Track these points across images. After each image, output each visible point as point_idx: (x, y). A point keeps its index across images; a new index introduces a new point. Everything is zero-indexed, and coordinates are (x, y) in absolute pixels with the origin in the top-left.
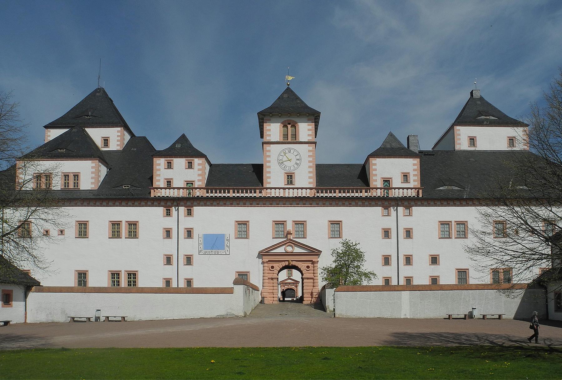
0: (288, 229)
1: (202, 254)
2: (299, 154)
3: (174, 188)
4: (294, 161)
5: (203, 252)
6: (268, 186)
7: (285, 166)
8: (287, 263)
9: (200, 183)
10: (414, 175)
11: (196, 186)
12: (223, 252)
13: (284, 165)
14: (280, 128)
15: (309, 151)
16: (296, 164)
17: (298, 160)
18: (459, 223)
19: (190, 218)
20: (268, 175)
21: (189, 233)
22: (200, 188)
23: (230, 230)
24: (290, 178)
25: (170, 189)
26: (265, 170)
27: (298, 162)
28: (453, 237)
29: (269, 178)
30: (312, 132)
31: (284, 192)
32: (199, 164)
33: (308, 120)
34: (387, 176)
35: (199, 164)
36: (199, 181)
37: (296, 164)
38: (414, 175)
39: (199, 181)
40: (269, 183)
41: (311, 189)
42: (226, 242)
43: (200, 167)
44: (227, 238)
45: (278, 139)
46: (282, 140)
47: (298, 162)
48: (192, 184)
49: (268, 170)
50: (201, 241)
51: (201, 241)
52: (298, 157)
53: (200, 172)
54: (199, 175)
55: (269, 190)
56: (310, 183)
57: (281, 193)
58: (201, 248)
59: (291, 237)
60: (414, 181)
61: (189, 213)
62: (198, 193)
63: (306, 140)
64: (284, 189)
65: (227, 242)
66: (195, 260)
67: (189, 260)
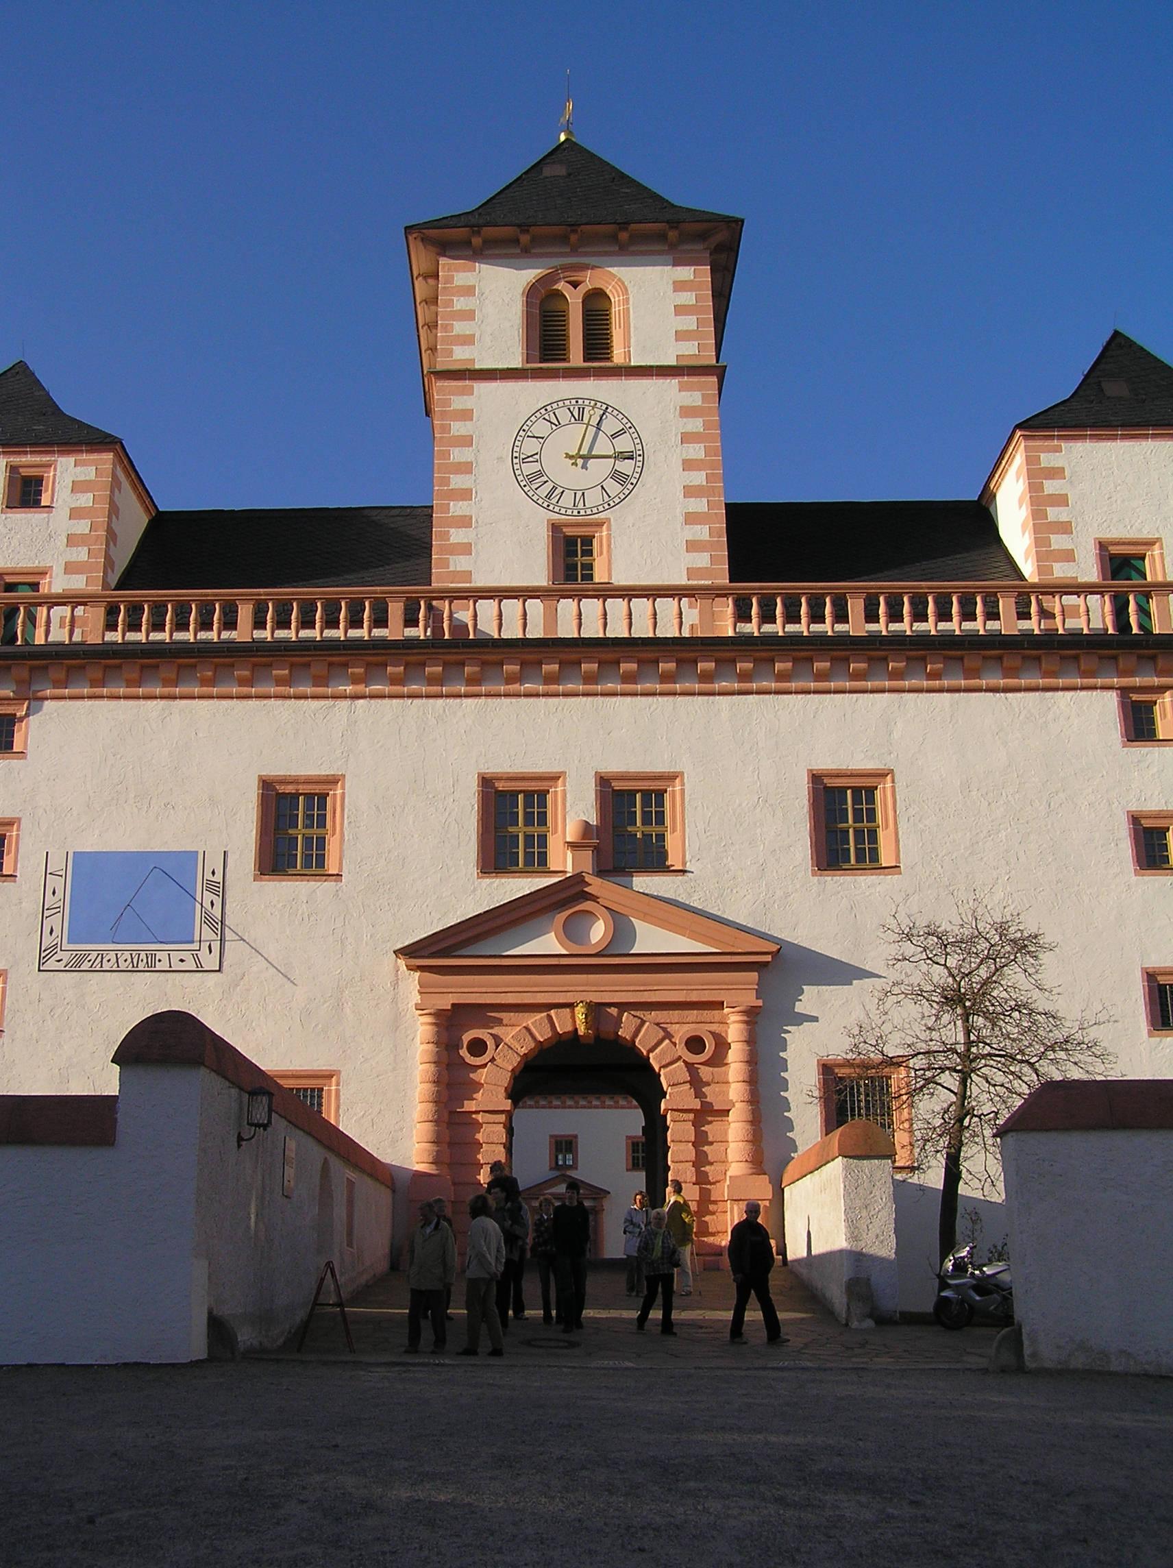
1: (61, 966)
5: (66, 956)
7: (554, 489)
12: (183, 955)
13: (550, 485)
15: (686, 412)
16: (617, 476)
20: (457, 536)
27: (626, 467)
30: (700, 322)
32: (77, 487)
34: (1122, 530)
35: (77, 487)
36: (70, 568)
37: (617, 476)
39: (70, 568)
40: (468, 575)
44: (208, 876)
45: (517, 362)
50: (60, 894)
51: (60, 894)
58: (57, 932)
65: (208, 897)
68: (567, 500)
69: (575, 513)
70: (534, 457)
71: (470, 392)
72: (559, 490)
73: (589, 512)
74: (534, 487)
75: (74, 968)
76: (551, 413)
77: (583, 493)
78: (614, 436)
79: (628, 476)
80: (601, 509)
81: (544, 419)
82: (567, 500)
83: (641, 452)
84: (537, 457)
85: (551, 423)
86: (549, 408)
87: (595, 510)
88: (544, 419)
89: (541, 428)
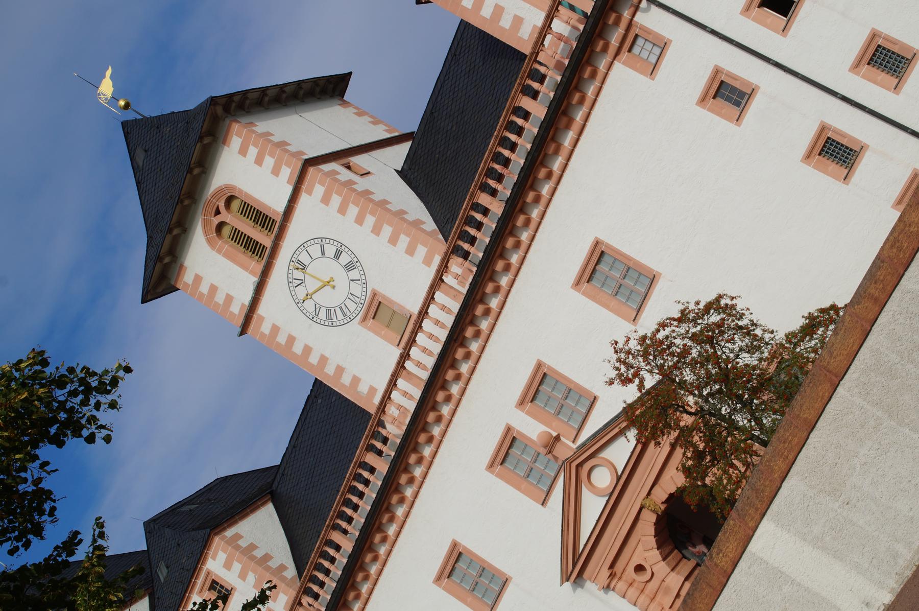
0: (534, 436)
2: (322, 241)
6: (377, 400)
8: (649, 518)
13: (338, 310)
14: (219, 251)
15: (326, 200)
16: (349, 267)
17: (338, 255)
27: (345, 259)
31: (411, 377)
33: (228, 146)
35: (228, 565)
40: (372, 390)
45: (251, 281)
46: (259, 268)
47: (345, 259)
52: (330, 250)
55: (392, 410)
59: (568, 446)
63: (289, 189)
68: (352, 306)
69: (361, 306)
71: (262, 319)
72: (343, 306)
73: (364, 298)
74: (335, 319)
76: (294, 281)
77: (351, 294)
78: (323, 253)
79: (351, 261)
80: (364, 290)
81: (296, 287)
82: (352, 306)
83: (340, 244)
84: (317, 306)
85: (300, 284)
86: (290, 280)
87: (364, 294)
88: (296, 287)
89: (301, 292)
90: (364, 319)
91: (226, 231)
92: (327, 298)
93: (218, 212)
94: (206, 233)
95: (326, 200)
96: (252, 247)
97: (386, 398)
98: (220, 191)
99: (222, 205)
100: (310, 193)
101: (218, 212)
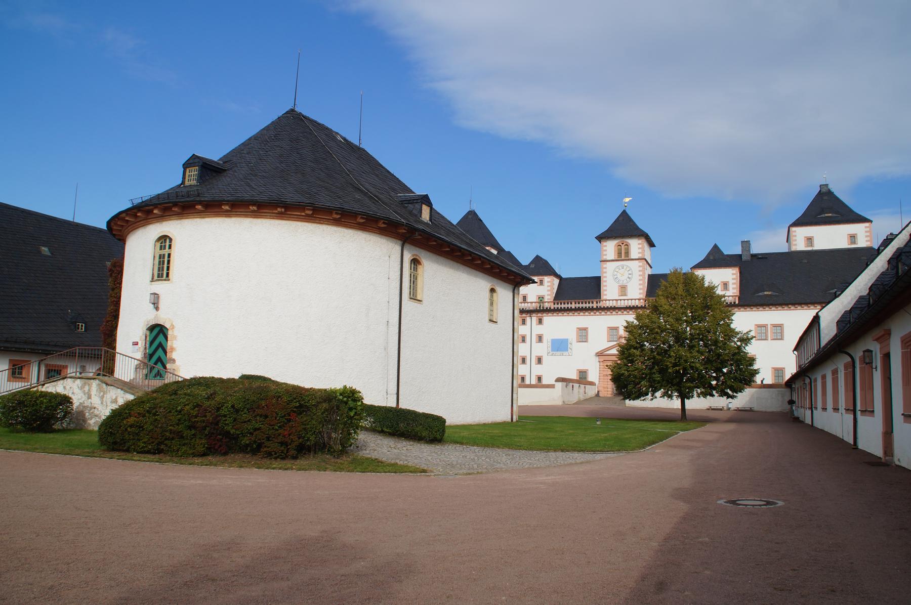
0: (620, 333)
3: (528, 303)
4: (626, 275)
9: (549, 297)
10: (733, 284)
11: (546, 301)
15: (640, 266)
16: (629, 277)
17: (630, 274)
18: (775, 326)
19: (540, 326)
21: (540, 338)
22: (549, 302)
23: (572, 336)
24: (623, 289)
25: (524, 303)
26: (603, 284)
28: (769, 338)
29: (606, 290)
31: (617, 303)
32: (548, 282)
35: (548, 282)
36: (548, 295)
37: (629, 277)
38: (733, 284)
39: (548, 295)
41: (639, 300)
42: (569, 345)
43: (549, 284)
45: (613, 258)
46: (617, 259)
48: (543, 298)
49: (604, 284)
52: (630, 272)
53: (549, 288)
54: (548, 291)
56: (640, 294)
57: (614, 304)
60: (733, 289)
61: (540, 321)
62: (547, 305)
63: (637, 258)
64: (617, 300)
66: (544, 360)
67: (539, 360)
68: (621, 282)
70: (616, 275)
71: (606, 264)
75: (552, 355)
82: (621, 282)
89: (617, 270)
90: (620, 286)
91: (619, 247)
92: (619, 276)
93: (623, 244)
94: (617, 243)
95: (640, 266)
96: (620, 254)
97: (606, 300)
98: (628, 242)
99: (625, 244)
100: (639, 262)
101: (623, 244)
